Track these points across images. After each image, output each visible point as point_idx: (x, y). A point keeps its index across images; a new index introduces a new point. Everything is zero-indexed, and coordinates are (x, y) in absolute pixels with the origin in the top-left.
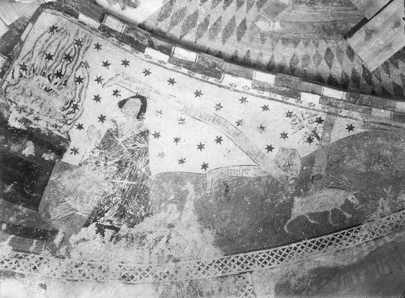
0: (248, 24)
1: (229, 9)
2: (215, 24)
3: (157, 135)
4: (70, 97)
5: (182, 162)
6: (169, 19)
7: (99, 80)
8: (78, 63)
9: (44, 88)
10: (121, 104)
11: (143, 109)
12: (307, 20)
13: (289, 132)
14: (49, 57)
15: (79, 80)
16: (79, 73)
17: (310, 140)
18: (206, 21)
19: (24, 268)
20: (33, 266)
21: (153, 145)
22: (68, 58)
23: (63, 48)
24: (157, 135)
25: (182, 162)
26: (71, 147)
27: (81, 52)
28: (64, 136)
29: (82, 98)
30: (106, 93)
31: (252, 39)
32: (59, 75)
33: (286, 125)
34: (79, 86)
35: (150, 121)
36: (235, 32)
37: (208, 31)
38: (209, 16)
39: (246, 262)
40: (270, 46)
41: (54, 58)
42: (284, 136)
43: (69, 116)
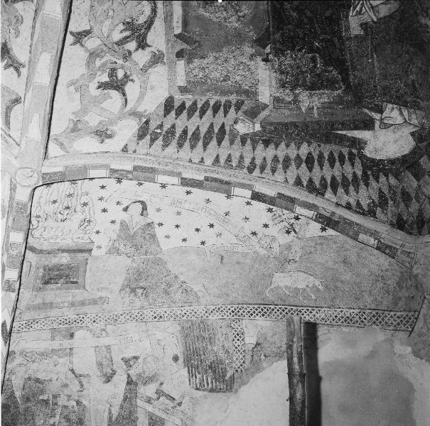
0: (227, 128)
1: (205, 118)
2: (194, 134)
3: (161, 225)
4: (83, 217)
5: (184, 240)
6: (148, 137)
7: (101, 199)
8: (80, 194)
9: (60, 220)
10: (126, 209)
11: (145, 208)
12: (290, 120)
13: (270, 223)
14: (55, 202)
15: (85, 204)
16: (84, 200)
17: (288, 232)
18: (185, 132)
21: (160, 232)
22: (70, 195)
23: (63, 192)
24: (161, 225)
25: (184, 240)
26: (96, 245)
27: (79, 188)
28: (89, 241)
29: (92, 215)
30: (111, 207)
31: (232, 142)
32: (68, 208)
33: (266, 217)
34: (86, 208)
35: (153, 216)
36: (215, 139)
37: (188, 141)
38: (187, 127)
39: (239, 312)
40: (251, 148)
41: (59, 201)
42: (266, 226)
43: (87, 228)
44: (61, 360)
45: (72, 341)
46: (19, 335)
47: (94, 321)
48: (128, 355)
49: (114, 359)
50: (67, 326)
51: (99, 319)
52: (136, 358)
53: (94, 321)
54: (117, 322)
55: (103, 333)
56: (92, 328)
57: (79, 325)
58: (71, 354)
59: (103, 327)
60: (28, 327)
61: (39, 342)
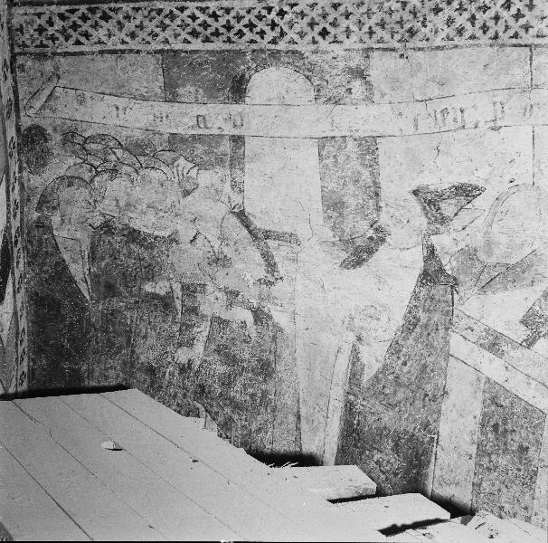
19: (296, 38)
20: (318, 29)
44: (205, 178)
45: (235, 109)
46: (48, 66)
47: (324, 33)
48: (439, 178)
49: (388, 190)
50: (218, 45)
51: (344, 23)
52: (466, 192)
53: (324, 33)
54: (416, 42)
55: (357, 85)
56: (314, 58)
57: (263, 43)
58: (236, 161)
59: (356, 61)
60: (75, 35)
61: (121, 102)
